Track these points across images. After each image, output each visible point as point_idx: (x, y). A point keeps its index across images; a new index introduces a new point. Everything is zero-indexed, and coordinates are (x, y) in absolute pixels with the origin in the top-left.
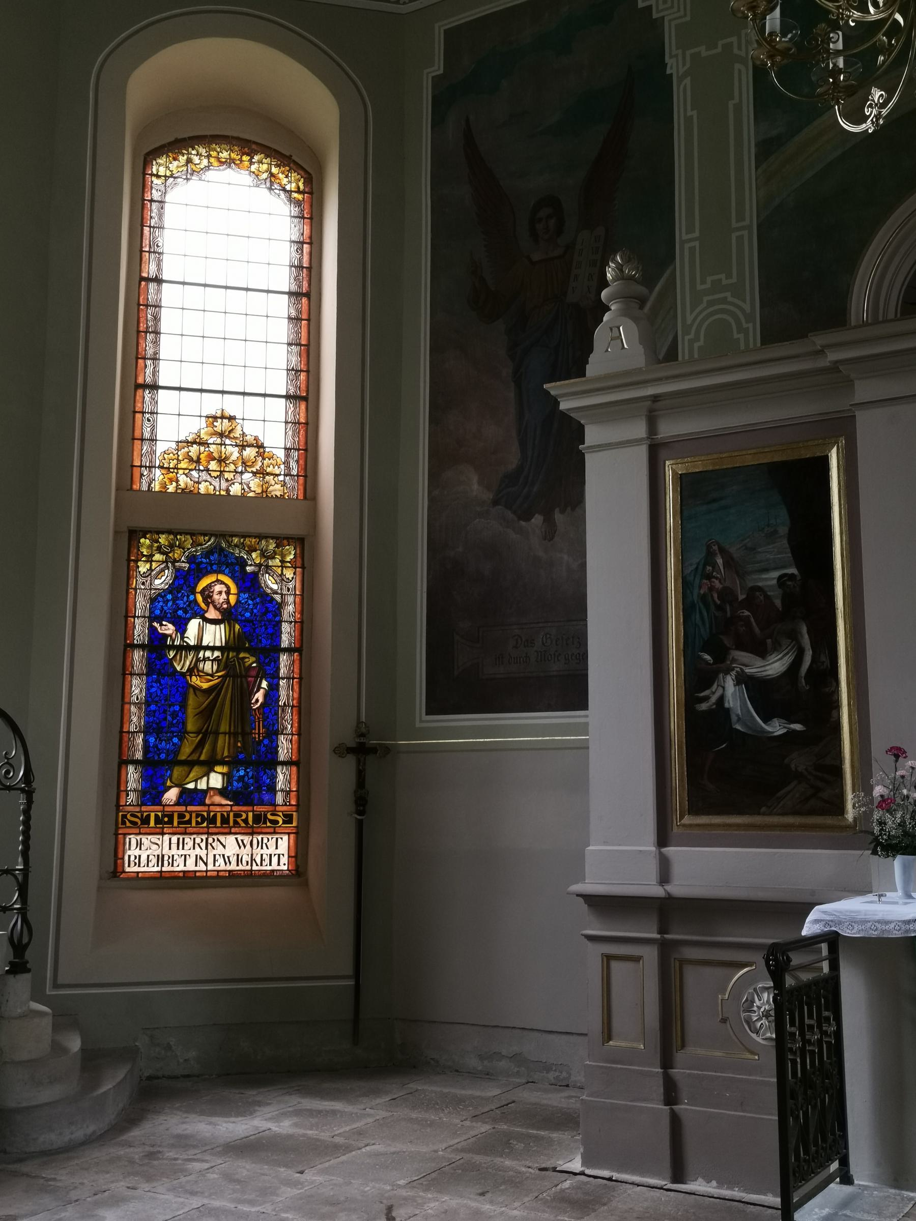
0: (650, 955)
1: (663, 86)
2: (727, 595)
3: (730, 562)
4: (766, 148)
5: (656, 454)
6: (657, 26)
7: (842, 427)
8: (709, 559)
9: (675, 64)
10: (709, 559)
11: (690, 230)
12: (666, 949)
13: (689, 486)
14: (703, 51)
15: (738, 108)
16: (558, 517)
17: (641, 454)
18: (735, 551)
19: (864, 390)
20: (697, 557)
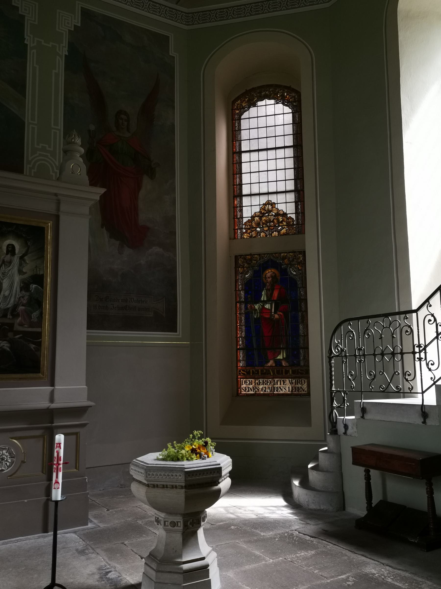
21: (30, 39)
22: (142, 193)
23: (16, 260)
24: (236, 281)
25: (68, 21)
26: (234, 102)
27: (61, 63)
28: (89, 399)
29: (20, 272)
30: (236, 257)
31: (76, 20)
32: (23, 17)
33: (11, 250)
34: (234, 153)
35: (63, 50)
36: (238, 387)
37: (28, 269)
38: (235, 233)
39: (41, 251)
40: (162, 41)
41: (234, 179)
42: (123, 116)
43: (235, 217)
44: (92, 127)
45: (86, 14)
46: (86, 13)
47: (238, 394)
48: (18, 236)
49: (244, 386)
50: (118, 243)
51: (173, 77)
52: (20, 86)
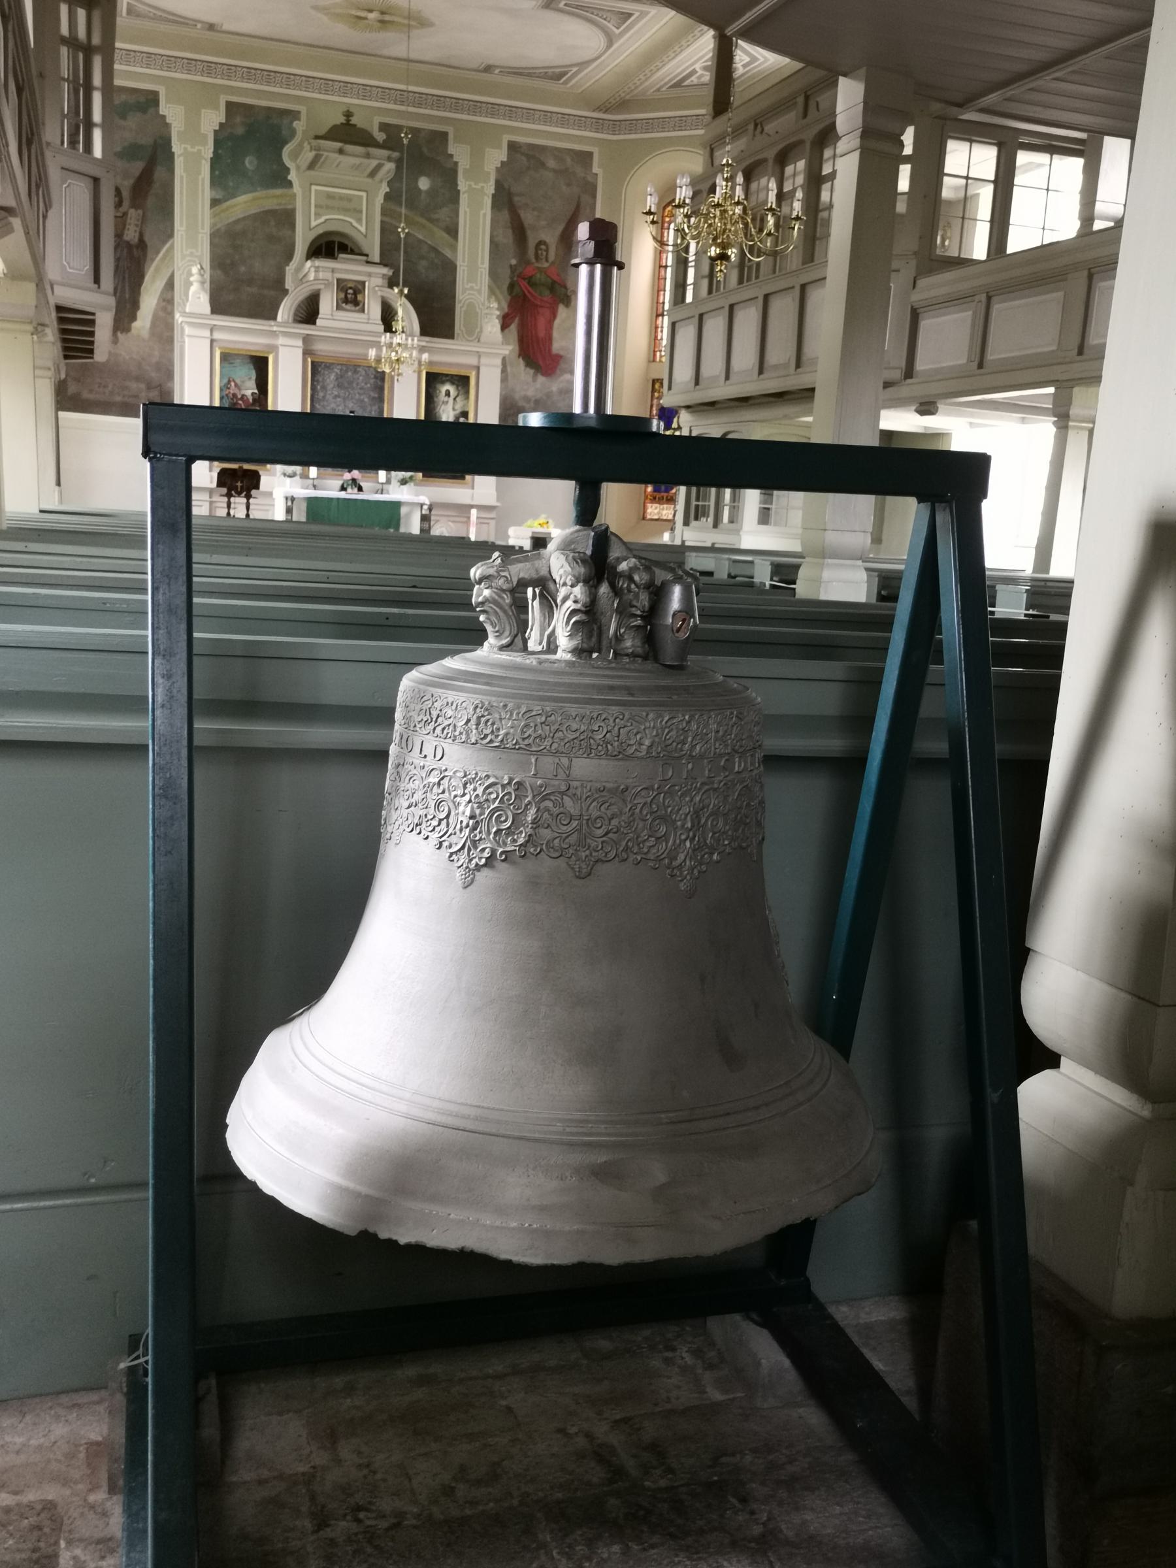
0: (207, 504)
1: (171, 156)
2: (234, 395)
3: (236, 385)
4: (215, 203)
5: (212, 341)
6: (167, 126)
7: (274, 349)
8: (229, 382)
9: (177, 147)
10: (229, 382)
11: (181, 225)
12: (211, 503)
13: (226, 357)
14: (189, 147)
15: (203, 179)
16: (119, 334)
17: (208, 342)
18: (238, 381)
19: (281, 341)
20: (225, 381)
21: (462, 185)
22: (557, 322)
23: (451, 400)
24: (652, 406)
25: (496, 157)
26: (664, 208)
27: (488, 202)
28: (498, 500)
29: (454, 409)
30: (654, 382)
31: (501, 155)
32: (456, 163)
33: (448, 394)
34: (660, 267)
35: (490, 189)
36: (645, 512)
37: (459, 407)
38: (655, 355)
39: (467, 392)
40: (585, 158)
41: (658, 296)
42: (543, 247)
43: (656, 337)
44: (514, 262)
45: (513, 147)
46: (513, 147)
47: (644, 518)
48: (453, 383)
49: (649, 511)
50: (532, 371)
51: (594, 197)
52: (453, 231)
